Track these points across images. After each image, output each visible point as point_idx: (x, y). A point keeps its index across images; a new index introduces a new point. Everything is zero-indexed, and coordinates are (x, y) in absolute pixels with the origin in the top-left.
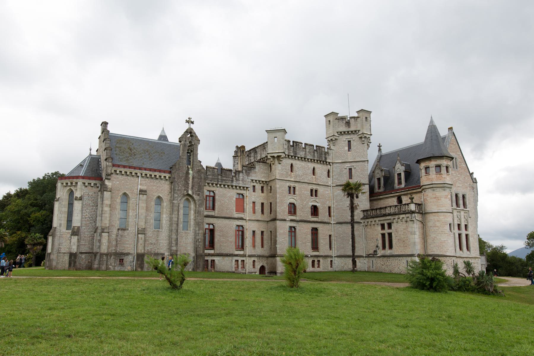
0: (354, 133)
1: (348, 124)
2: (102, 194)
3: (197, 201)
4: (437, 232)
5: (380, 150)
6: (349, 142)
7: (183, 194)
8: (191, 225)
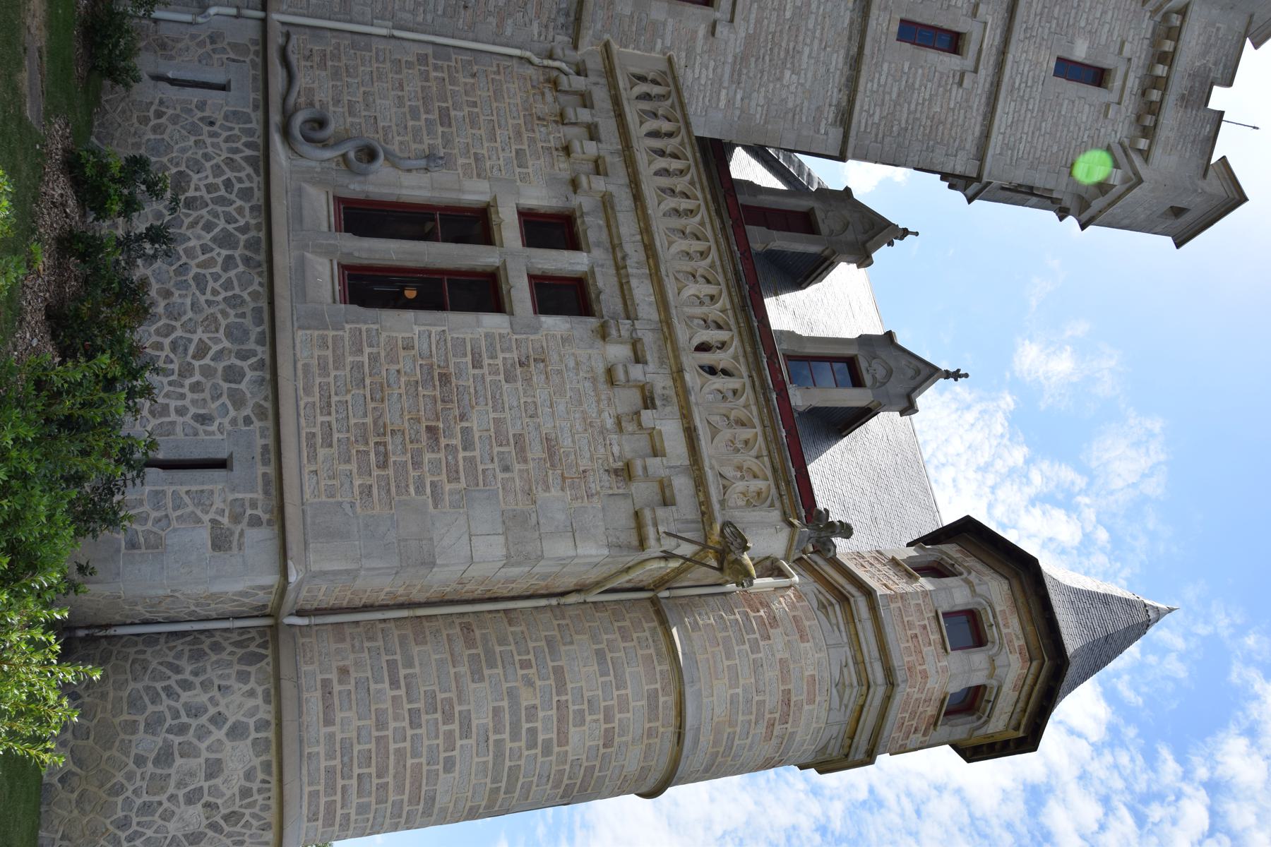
4: (515, 736)
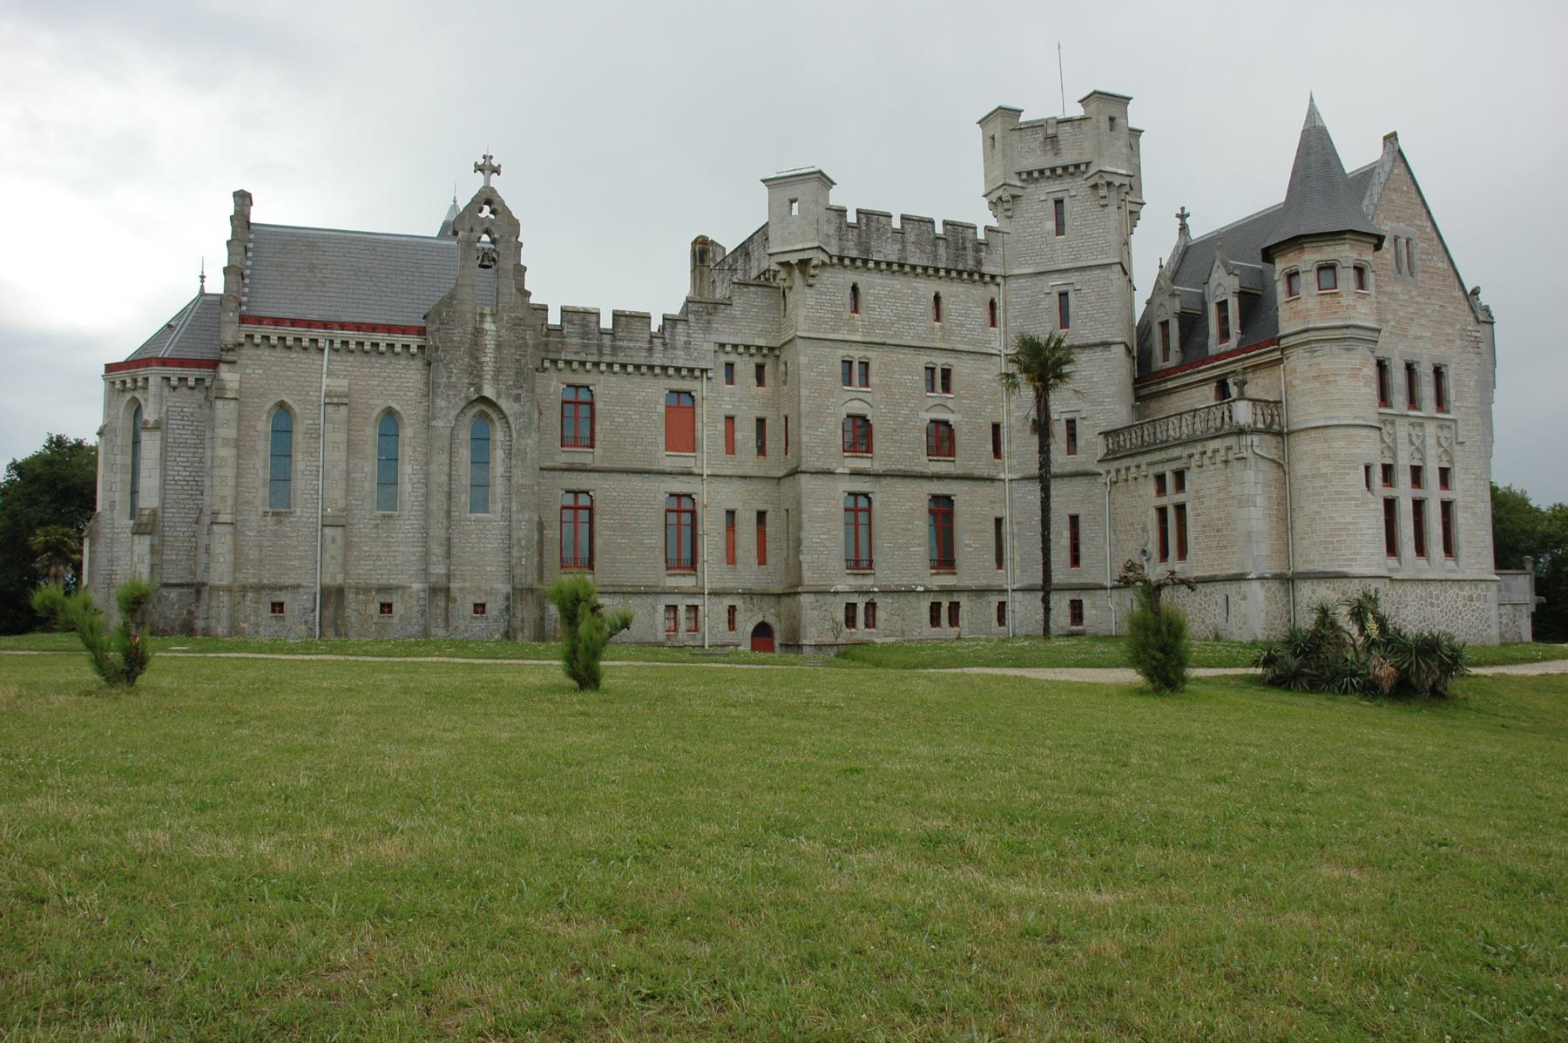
0: (1072, 174)
1: (1053, 140)
2: (211, 406)
3: (511, 420)
4: (1320, 494)
5: (1184, 228)
6: (1059, 202)
7: (467, 397)
8: (498, 495)
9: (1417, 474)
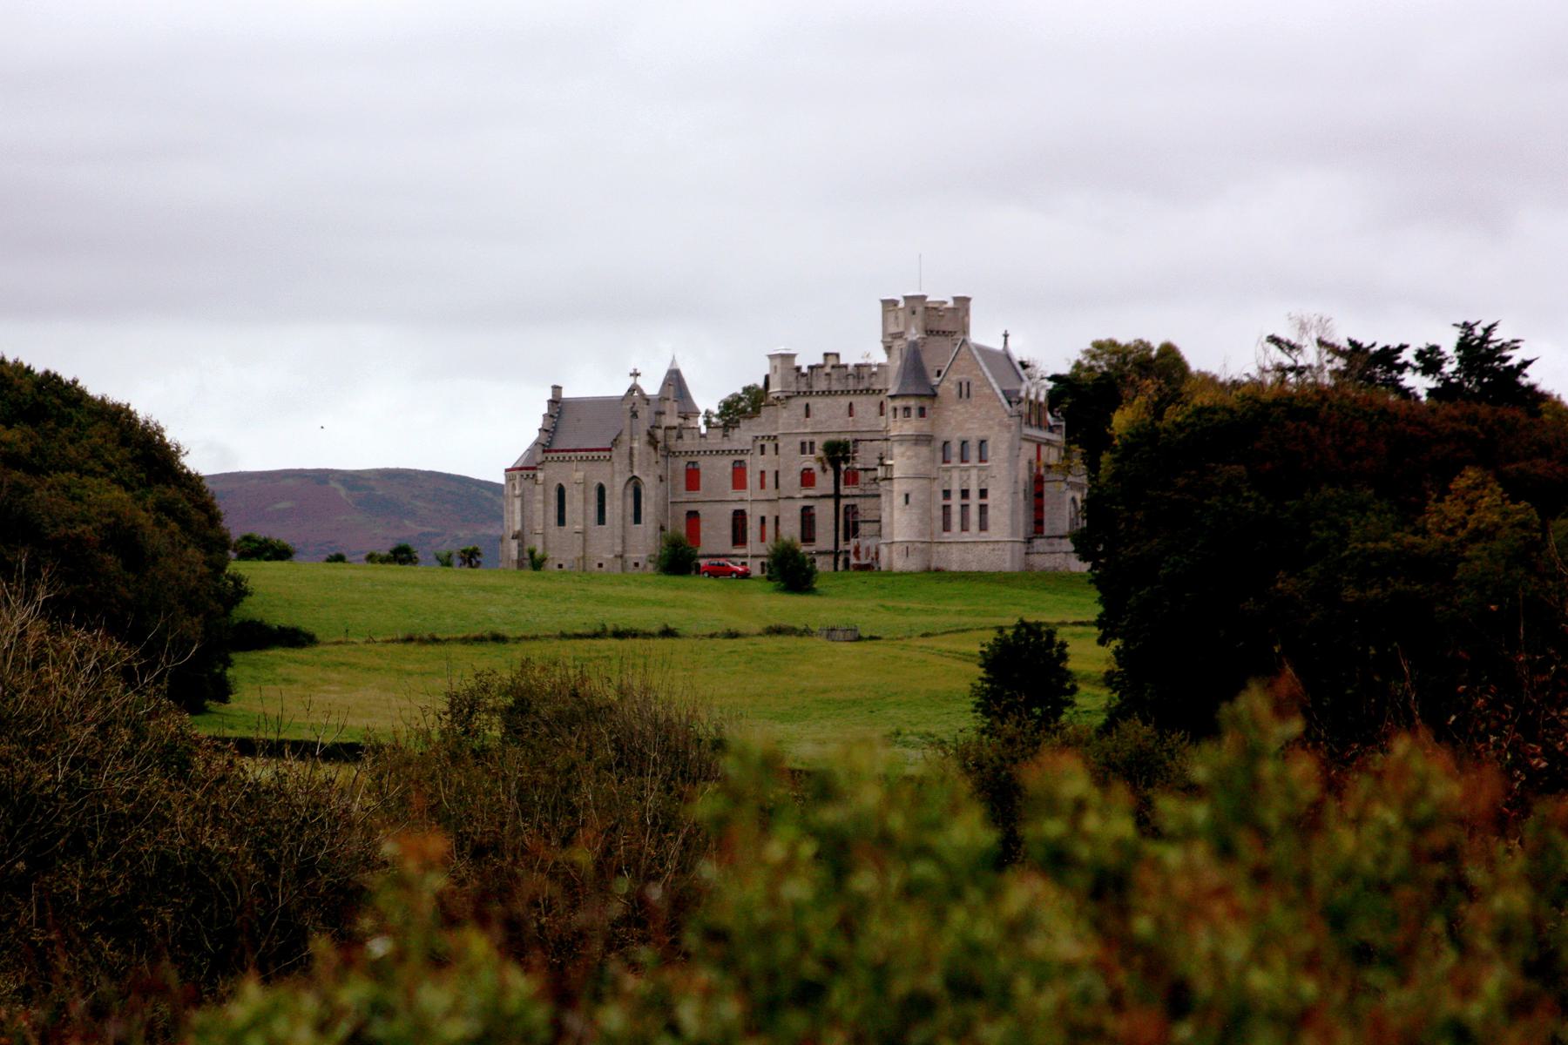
9: (965, 494)
